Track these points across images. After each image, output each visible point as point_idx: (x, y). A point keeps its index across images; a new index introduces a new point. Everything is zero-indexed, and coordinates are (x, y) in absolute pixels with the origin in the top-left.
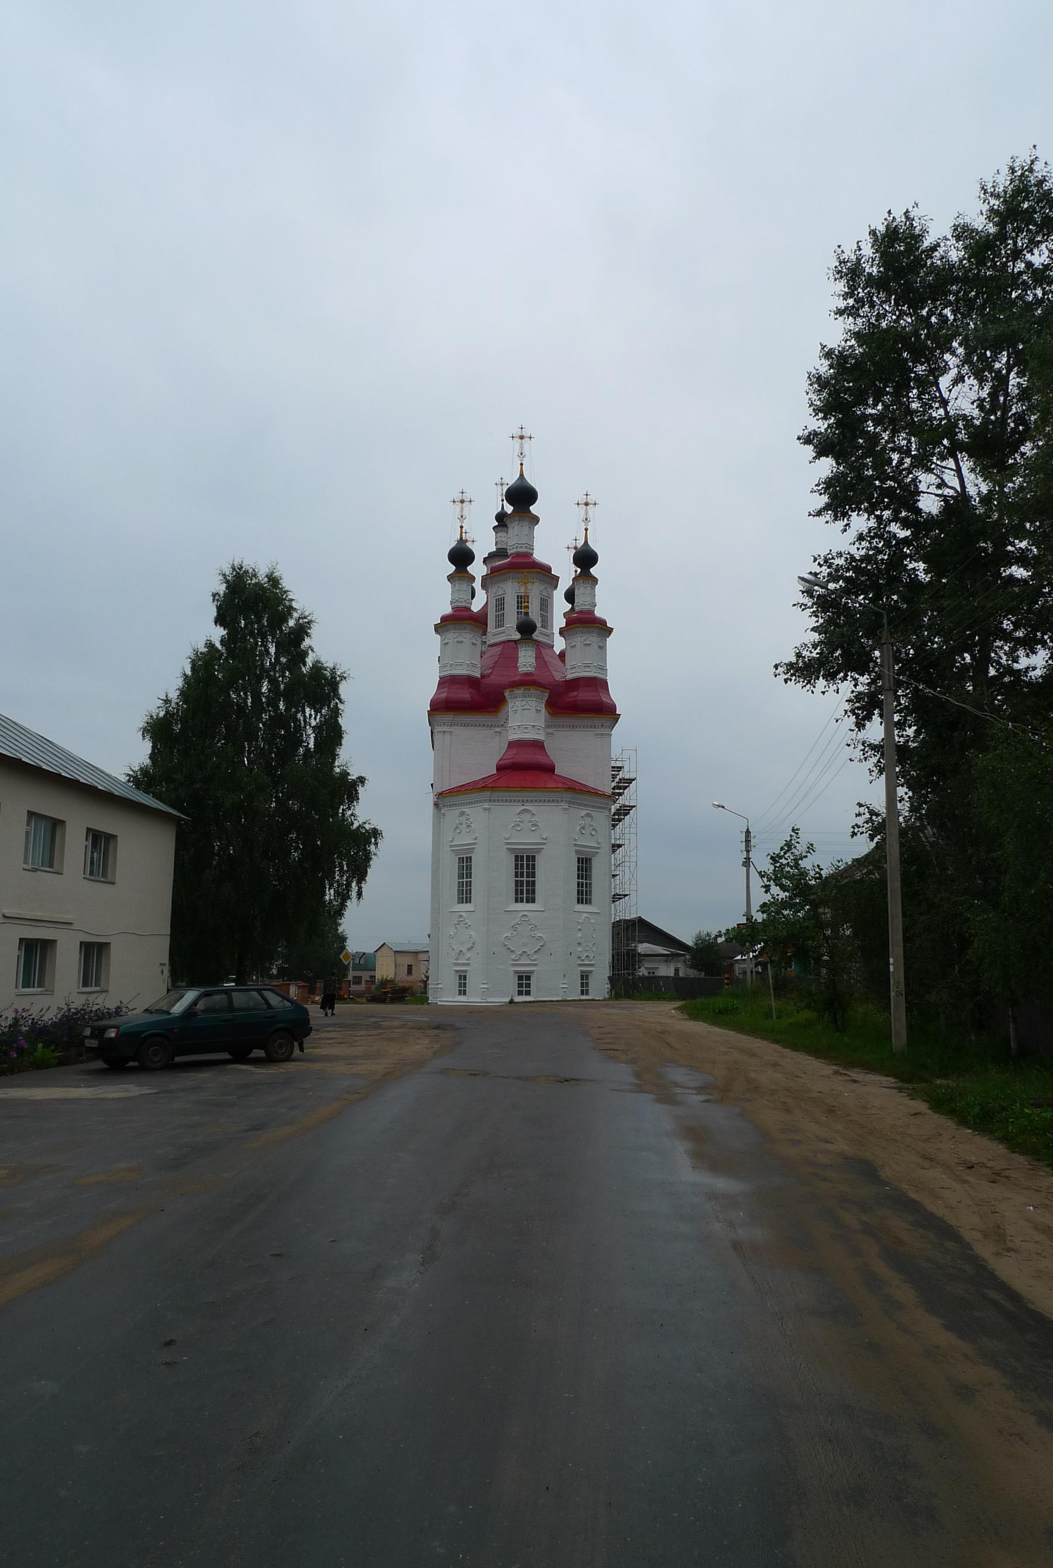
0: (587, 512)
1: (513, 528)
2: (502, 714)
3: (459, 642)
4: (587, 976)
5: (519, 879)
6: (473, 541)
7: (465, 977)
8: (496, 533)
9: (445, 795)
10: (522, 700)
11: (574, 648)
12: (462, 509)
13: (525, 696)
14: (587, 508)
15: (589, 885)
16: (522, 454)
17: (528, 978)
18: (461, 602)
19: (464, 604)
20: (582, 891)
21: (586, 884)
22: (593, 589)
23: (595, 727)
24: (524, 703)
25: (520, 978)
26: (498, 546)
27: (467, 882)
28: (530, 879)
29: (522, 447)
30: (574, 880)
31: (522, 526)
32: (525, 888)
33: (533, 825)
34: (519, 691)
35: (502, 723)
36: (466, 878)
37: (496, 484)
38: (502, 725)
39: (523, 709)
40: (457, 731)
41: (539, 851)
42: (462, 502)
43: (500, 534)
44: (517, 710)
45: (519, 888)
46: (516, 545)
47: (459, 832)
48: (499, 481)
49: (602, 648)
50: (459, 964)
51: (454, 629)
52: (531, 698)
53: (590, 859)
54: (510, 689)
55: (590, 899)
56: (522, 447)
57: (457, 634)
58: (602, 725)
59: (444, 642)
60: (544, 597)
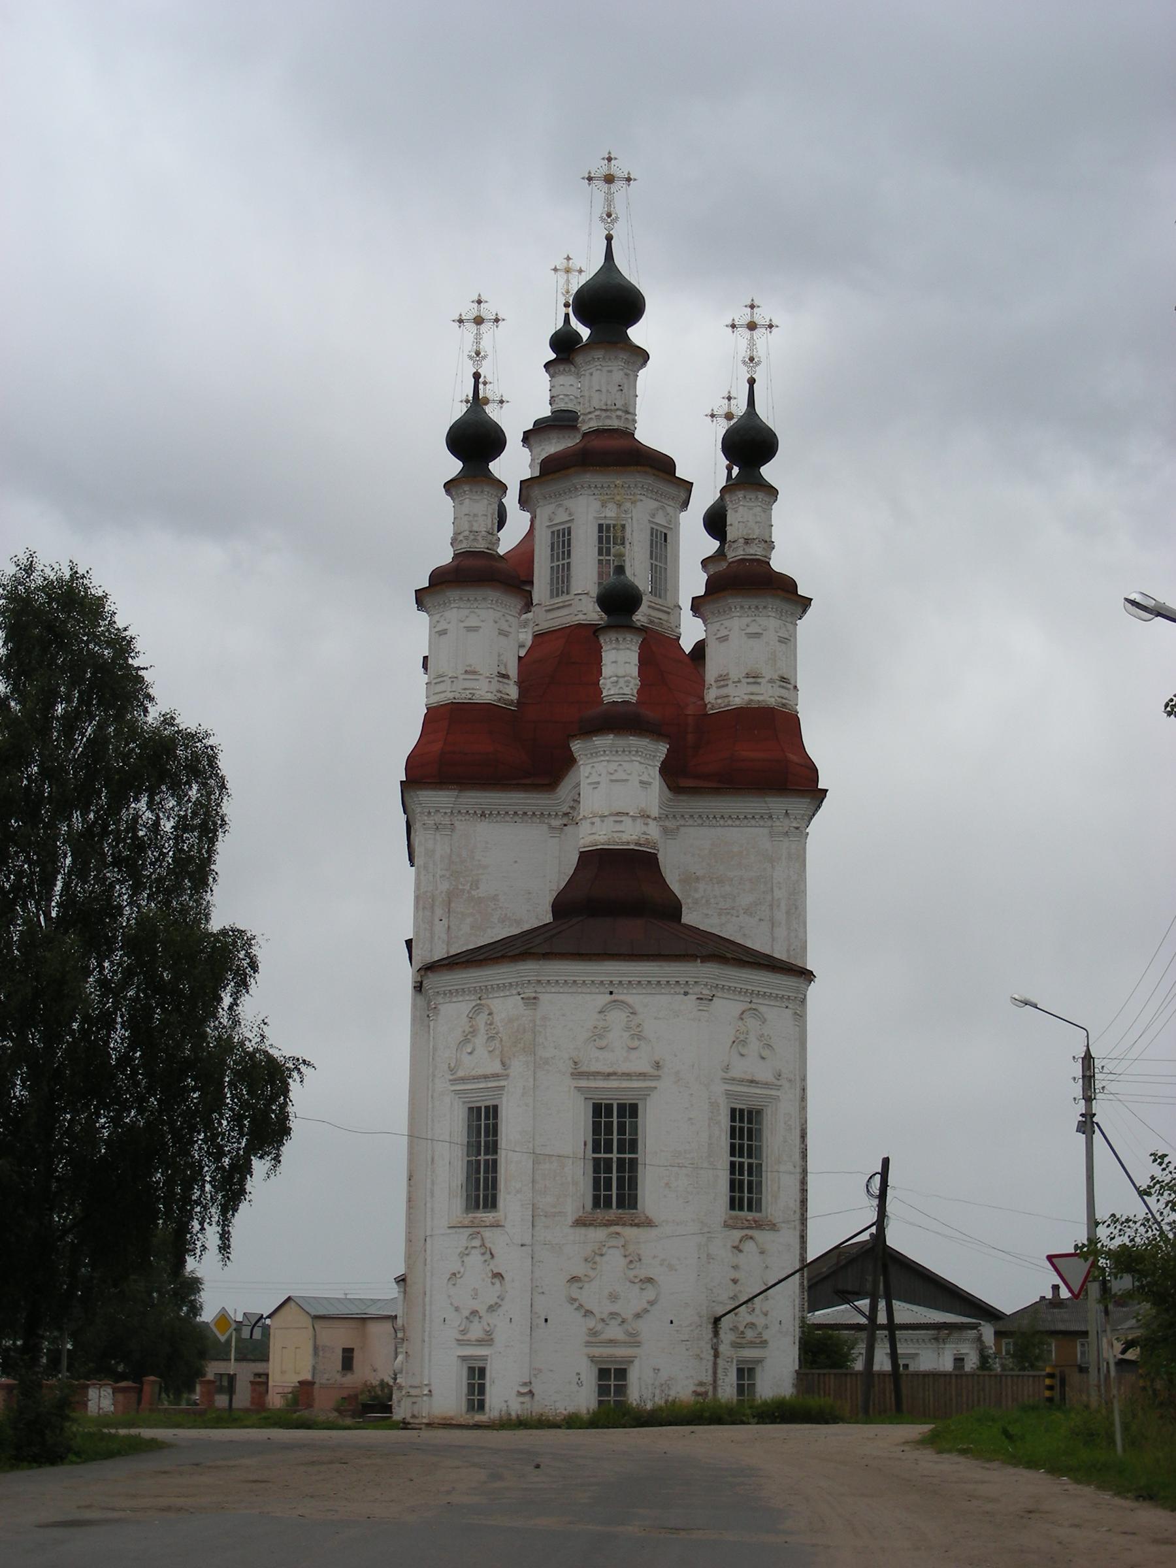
0: (752, 344)
1: (591, 374)
2: (564, 790)
3: (470, 629)
4: (751, 1371)
5: (602, 1155)
6: (502, 402)
7: (482, 1371)
8: (552, 376)
10: (608, 761)
11: (725, 644)
12: (478, 338)
14: (752, 337)
15: (755, 1170)
16: (609, 215)
20: (741, 1182)
21: (750, 1165)
22: (768, 510)
23: (771, 817)
24: (614, 766)
26: (557, 407)
27: (486, 1161)
28: (627, 1156)
29: (609, 201)
30: (724, 1159)
31: (610, 371)
32: (614, 1175)
33: (632, 1037)
34: (603, 741)
35: (565, 809)
36: (486, 1153)
37: (555, 270)
38: (566, 814)
39: (612, 781)
42: (479, 321)
43: (561, 379)
44: (598, 783)
45: (602, 1175)
47: (469, 1051)
48: (561, 263)
49: (788, 641)
51: (461, 599)
53: (759, 1112)
55: (759, 1201)
56: (609, 201)
57: (466, 612)
59: (436, 630)
60: (659, 528)
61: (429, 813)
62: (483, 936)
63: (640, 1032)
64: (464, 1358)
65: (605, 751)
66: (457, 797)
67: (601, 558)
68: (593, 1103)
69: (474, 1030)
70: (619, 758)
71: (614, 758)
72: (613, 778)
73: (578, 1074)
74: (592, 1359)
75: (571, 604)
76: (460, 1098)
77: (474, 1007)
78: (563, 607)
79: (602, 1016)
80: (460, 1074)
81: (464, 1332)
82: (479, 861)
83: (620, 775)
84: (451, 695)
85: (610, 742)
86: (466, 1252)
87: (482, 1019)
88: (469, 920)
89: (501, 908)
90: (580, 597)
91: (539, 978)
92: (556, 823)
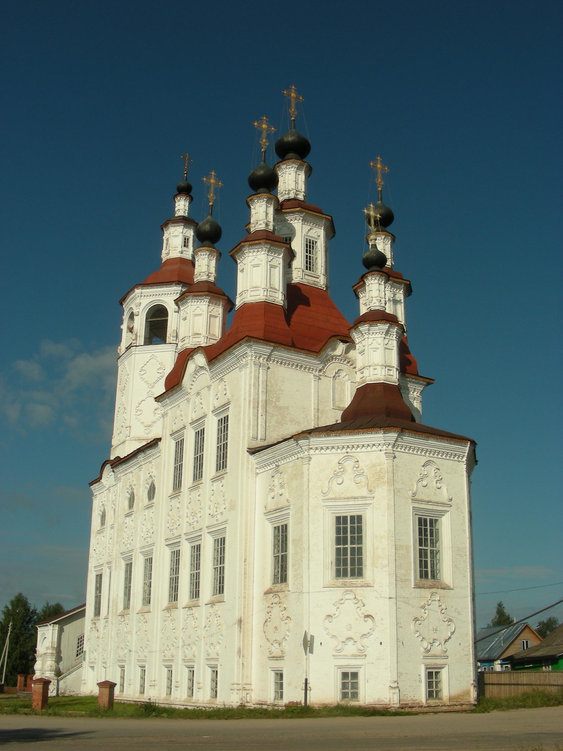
7: (355, 675)
47: (340, 482)
50: (346, 657)
62: (282, 428)
67: (307, 254)
69: (343, 471)
72: (387, 347)
73: (414, 500)
77: (344, 457)
82: (280, 387)
88: (275, 418)
89: (290, 414)
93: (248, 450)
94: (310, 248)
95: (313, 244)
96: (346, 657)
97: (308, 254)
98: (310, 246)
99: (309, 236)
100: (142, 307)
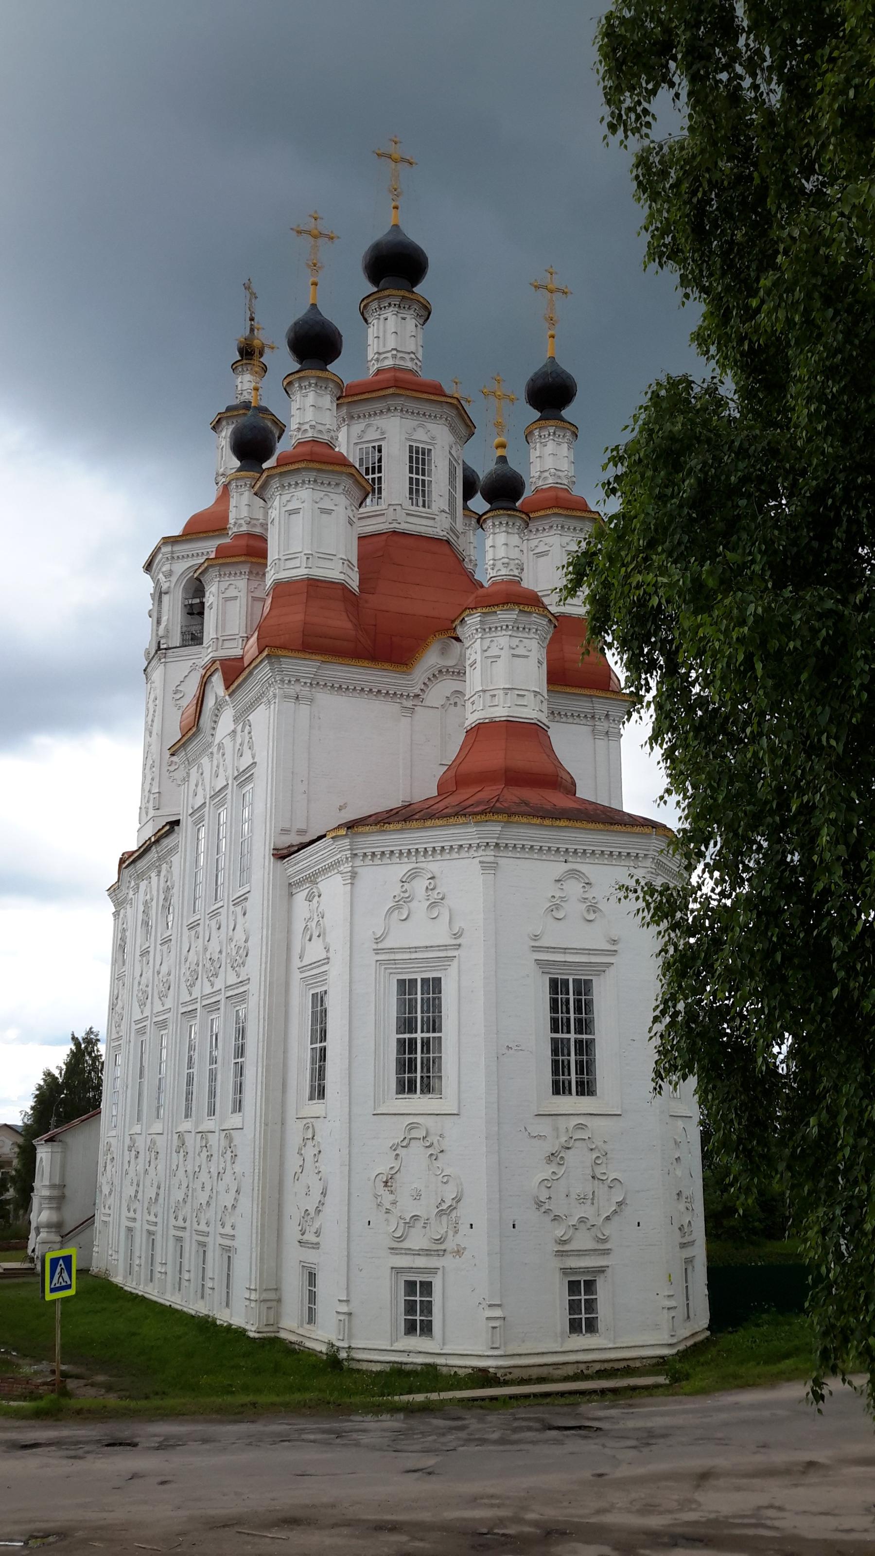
3: (323, 511)
7: (427, 1287)
9: (361, 829)
13: (518, 628)
17: (590, 1286)
18: (320, 431)
19: (326, 437)
24: (515, 642)
25: (573, 1287)
31: (404, 319)
35: (417, 691)
39: (514, 656)
40: (326, 700)
41: (602, 969)
44: (499, 657)
46: (394, 352)
50: (409, 1252)
52: (529, 633)
54: (484, 610)
58: (607, 715)
61: (290, 681)
63: (596, 903)
64: (397, 1271)
65: (507, 626)
66: (319, 668)
67: (411, 475)
68: (550, 979)
70: (520, 635)
71: (515, 634)
72: (516, 652)
74: (565, 1271)
75: (384, 514)
76: (386, 968)
78: (373, 516)
79: (559, 885)
80: (387, 944)
81: (401, 1239)
83: (520, 651)
84: (306, 571)
85: (515, 616)
86: (404, 1144)
87: (420, 885)
90: (395, 507)
91: (499, 841)
92: (409, 704)
93: (275, 852)
94: (417, 463)
95: (423, 454)
96: (409, 1252)
97: (414, 476)
98: (417, 458)
99: (416, 441)
100: (174, 579)
